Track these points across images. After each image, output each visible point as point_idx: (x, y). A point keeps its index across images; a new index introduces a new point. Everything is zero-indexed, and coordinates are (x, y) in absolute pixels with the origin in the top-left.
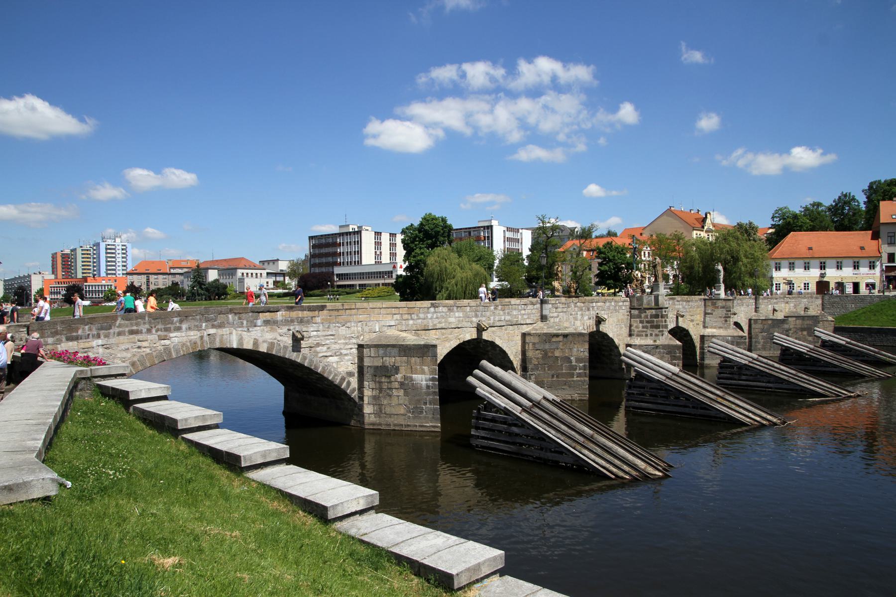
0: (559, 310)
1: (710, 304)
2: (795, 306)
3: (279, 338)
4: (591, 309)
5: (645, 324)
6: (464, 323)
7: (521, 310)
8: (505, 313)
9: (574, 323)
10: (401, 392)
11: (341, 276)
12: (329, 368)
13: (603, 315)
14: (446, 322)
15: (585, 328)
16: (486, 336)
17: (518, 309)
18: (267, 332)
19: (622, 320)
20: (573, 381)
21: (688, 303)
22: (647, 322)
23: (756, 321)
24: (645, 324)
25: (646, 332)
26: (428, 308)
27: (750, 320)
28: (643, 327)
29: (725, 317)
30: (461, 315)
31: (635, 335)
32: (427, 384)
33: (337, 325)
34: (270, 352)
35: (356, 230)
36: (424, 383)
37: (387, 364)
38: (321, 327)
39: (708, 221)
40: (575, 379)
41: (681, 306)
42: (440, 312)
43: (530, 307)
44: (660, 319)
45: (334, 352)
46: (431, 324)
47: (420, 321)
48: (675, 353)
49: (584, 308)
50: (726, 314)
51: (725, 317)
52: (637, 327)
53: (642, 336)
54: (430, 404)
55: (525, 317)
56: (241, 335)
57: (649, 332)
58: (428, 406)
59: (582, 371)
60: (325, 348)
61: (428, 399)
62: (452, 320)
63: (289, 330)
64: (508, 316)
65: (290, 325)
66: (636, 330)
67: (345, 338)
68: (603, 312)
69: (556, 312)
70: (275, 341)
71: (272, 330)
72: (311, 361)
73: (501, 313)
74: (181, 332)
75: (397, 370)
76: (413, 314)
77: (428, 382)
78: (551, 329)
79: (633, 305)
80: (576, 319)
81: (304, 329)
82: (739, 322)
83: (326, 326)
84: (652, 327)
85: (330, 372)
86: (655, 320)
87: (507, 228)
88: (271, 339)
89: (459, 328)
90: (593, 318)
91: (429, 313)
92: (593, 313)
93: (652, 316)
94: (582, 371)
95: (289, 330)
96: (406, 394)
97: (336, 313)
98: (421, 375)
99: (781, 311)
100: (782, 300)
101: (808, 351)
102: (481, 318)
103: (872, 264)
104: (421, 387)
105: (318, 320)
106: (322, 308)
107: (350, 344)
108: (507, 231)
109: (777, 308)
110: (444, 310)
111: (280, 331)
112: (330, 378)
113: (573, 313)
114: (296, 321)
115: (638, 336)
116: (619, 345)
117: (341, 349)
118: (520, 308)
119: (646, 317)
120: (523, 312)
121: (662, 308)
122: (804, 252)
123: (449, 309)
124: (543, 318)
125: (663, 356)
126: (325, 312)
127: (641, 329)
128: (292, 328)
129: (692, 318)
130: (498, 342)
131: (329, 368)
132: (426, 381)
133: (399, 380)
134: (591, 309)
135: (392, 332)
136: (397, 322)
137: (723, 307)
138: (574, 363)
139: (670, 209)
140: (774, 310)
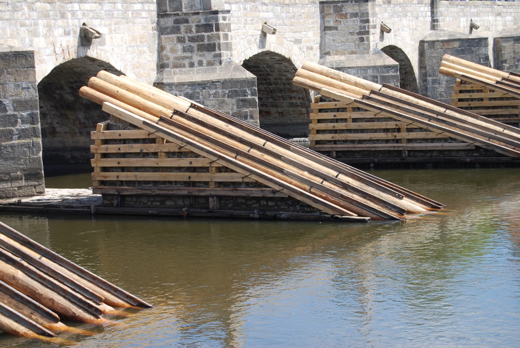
1: (332, 11)
4: (69, 15)
15: (58, 51)
19: (142, 37)
20: (12, 146)
21: (285, 9)
22: (192, 40)
23: (432, 43)
27: (422, 43)
28: (184, 50)
29: (359, 33)
40: (15, 142)
41: (270, 15)
44: (215, 32)
48: (245, 94)
49: (51, 13)
50: (360, 27)
51: (359, 33)
53: (184, 66)
57: (196, 59)
59: (27, 126)
80: (35, 34)
82: (399, 45)
84: (201, 48)
86: (206, 34)
90: (75, 33)
92: (75, 25)
94: (27, 126)
100: (490, 10)
101: (498, 82)
109: (478, 24)
113: (28, 22)
115: (175, 66)
121: (216, 12)
125: (223, 102)
127: (180, 53)
129: (298, 36)
137: (355, 15)
138: (10, 112)
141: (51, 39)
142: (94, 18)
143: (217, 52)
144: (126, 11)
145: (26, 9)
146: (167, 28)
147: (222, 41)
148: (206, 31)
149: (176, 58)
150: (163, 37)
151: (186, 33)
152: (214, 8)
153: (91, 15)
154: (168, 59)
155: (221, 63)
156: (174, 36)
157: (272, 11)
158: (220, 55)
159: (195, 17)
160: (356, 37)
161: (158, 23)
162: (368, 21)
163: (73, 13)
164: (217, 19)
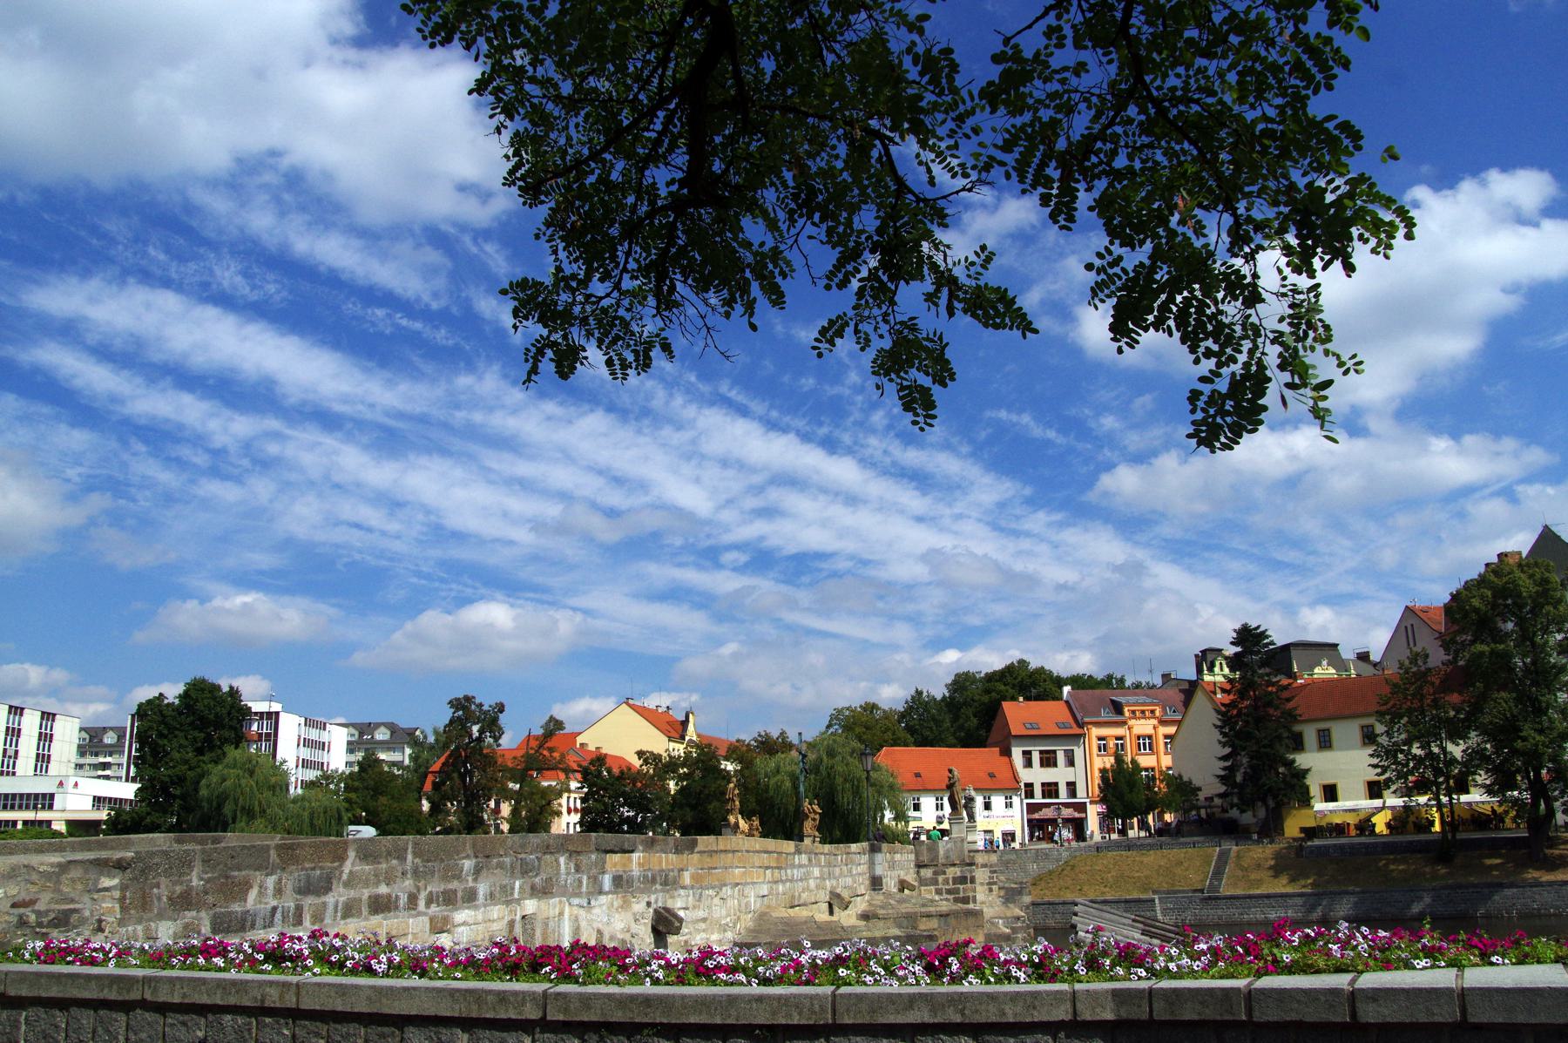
3: (635, 928)
5: (945, 896)
22: (949, 892)
29: (989, 884)
56: (576, 919)
63: (649, 904)
74: (476, 908)
93: (957, 880)
119: (946, 881)
137: (984, 866)
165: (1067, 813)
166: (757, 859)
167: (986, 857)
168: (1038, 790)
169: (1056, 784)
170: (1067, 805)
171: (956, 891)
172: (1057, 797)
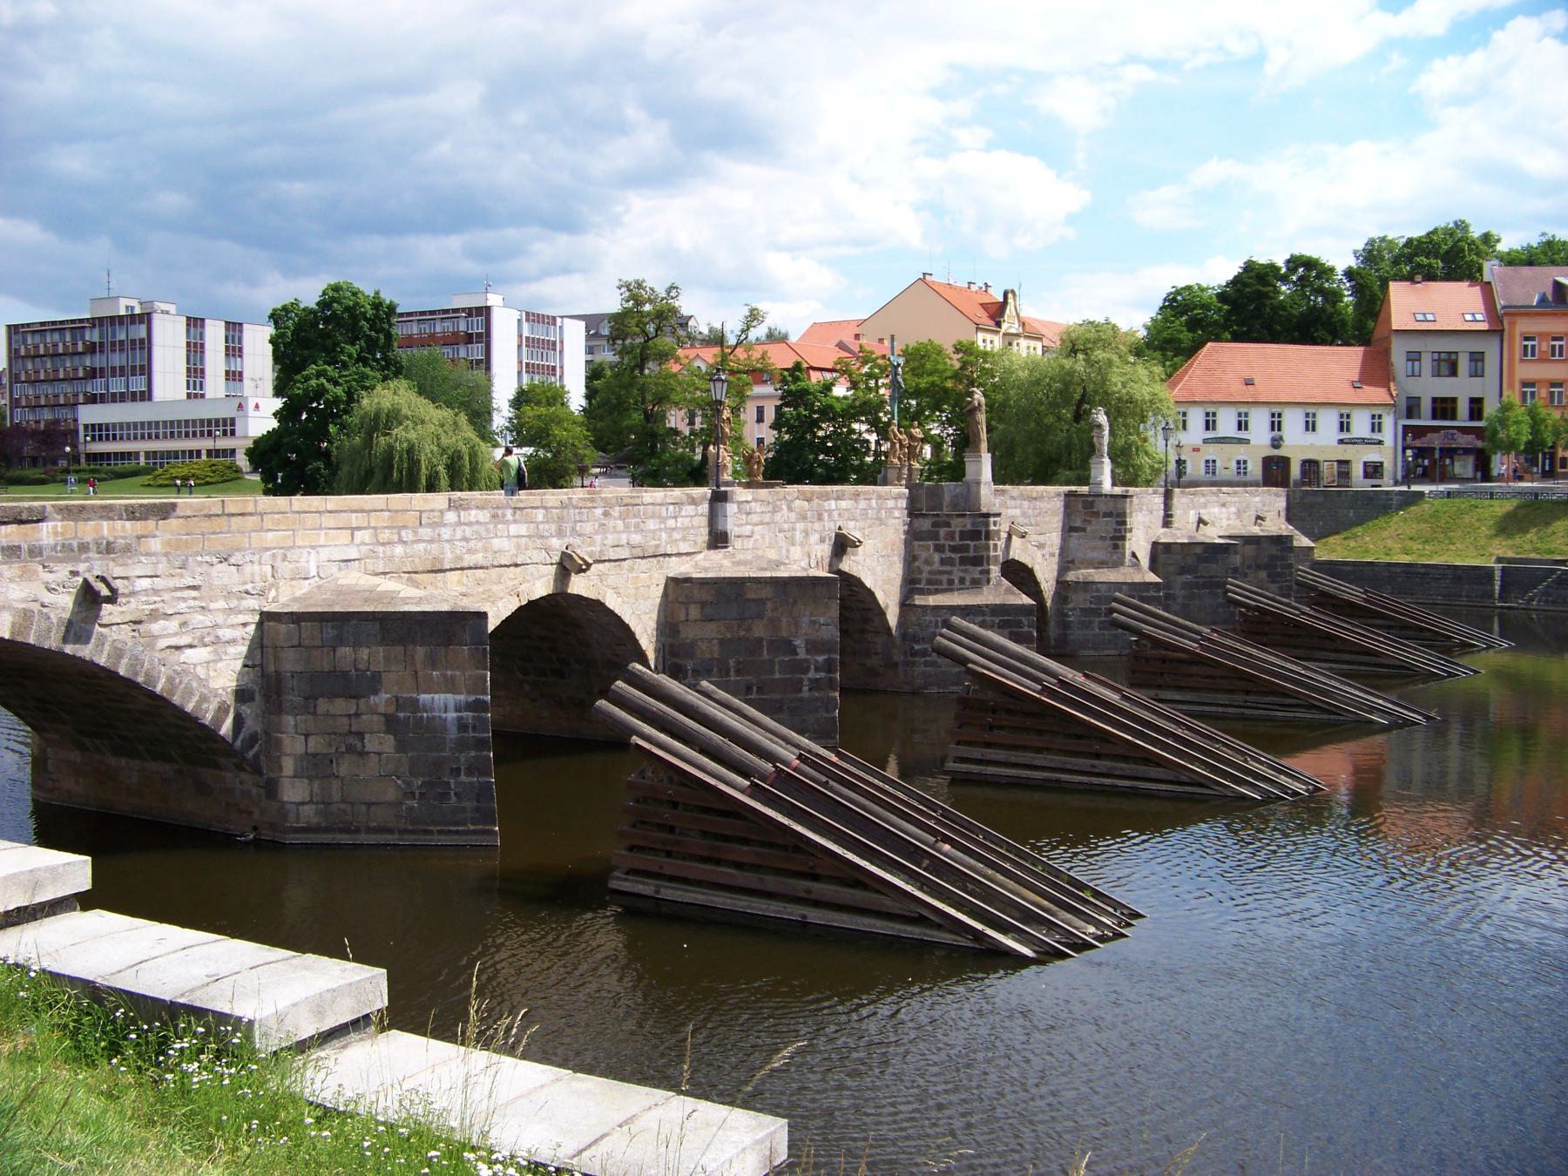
0: (755, 518)
2: (1239, 514)
3: (48, 598)
4: (826, 515)
5: (948, 554)
6: (529, 553)
7: (667, 518)
8: (627, 526)
9: (788, 551)
10: (389, 742)
11: (100, 431)
12: (185, 681)
13: (853, 530)
14: (486, 550)
16: (579, 586)
17: (660, 517)
18: (11, 580)
22: (953, 549)
23: (1168, 546)
24: (948, 554)
25: (950, 573)
26: (441, 512)
28: (943, 562)
29: (1113, 538)
30: (522, 529)
31: (924, 582)
32: (460, 719)
33: (207, 558)
34: (19, 639)
35: (137, 311)
36: (452, 715)
37: (346, 665)
38: (162, 568)
39: (1010, 310)
41: (1017, 512)
42: (470, 524)
43: (689, 510)
45: (198, 634)
46: (449, 555)
47: (421, 546)
48: (1019, 624)
49: (809, 514)
50: (1115, 530)
52: (928, 562)
54: (470, 772)
55: (676, 536)
58: (463, 778)
59: (822, 675)
60: (173, 625)
61: (462, 759)
62: (497, 543)
63: (74, 573)
64: (636, 532)
65: (76, 560)
66: (926, 568)
67: (229, 595)
68: (852, 524)
69: (747, 524)
70: (36, 607)
71: (26, 576)
72: (136, 661)
73: (620, 523)
75: (373, 683)
76: (405, 527)
77: (464, 714)
78: (742, 568)
79: (919, 506)
81: (118, 571)
83: (177, 564)
84: (963, 561)
85: (189, 692)
86: (972, 544)
87: (528, 314)
88: (24, 600)
89: (516, 565)
91: (445, 525)
92: (830, 528)
93: (963, 535)
94: (822, 675)
95: (74, 573)
96: (401, 746)
97: (205, 525)
98: (443, 696)
99: (1213, 525)
102: (571, 540)
103: (1376, 421)
104: (444, 729)
105: (155, 545)
106: (165, 512)
107: (240, 612)
108: (527, 320)
109: (1205, 518)
110: (481, 519)
111: (49, 577)
112: (189, 708)
114: (93, 547)
116: (887, 606)
117: (216, 626)
118: (664, 514)
119: (951, 536)
120: (671, 523)
121: (987, 515)
122: (1239, 392)
123: (494, 516)
124: (718, 539)
126: (173, 523)
127: (937, 566)
128: (82, 567)
129: (1042, 539)
130: (612, 603)
131: (185, 681)
132: (457, 709)
133: (382, 709)
134: (826, 515)
135: (355, 578)
136: (364, 548)
137: (1108, 514)
139: (923, 279)
140: (1201, 521)
141: (807, 548)
142: (849, 519)
143: (985, 567)
144: (880, 509)
145: (785, 507)
146: (922, 532)
147: (992, 553)
148: (972, 540)
149: (930, 572)
150: (916, 543)
151: (946, 539)
152: (984, 510)
153: (847, 514)
154: (921, 572)
155: (988, 582)
156: (930, 543)
157: (1020, 507)
158: (988, 572)
159: (960, 520)
160: (1109, 542)
161: (910, 524)
162: (1124, 523)
163: (830, 512)
164: (987, 524)
165: (1464, 441)
166: (328, 521)
167: (1111, 504)
168: (1426, 406)
169: (1454, 400)
170: (1464, 430)
171: (965, 548)
172: (1453, 417)
